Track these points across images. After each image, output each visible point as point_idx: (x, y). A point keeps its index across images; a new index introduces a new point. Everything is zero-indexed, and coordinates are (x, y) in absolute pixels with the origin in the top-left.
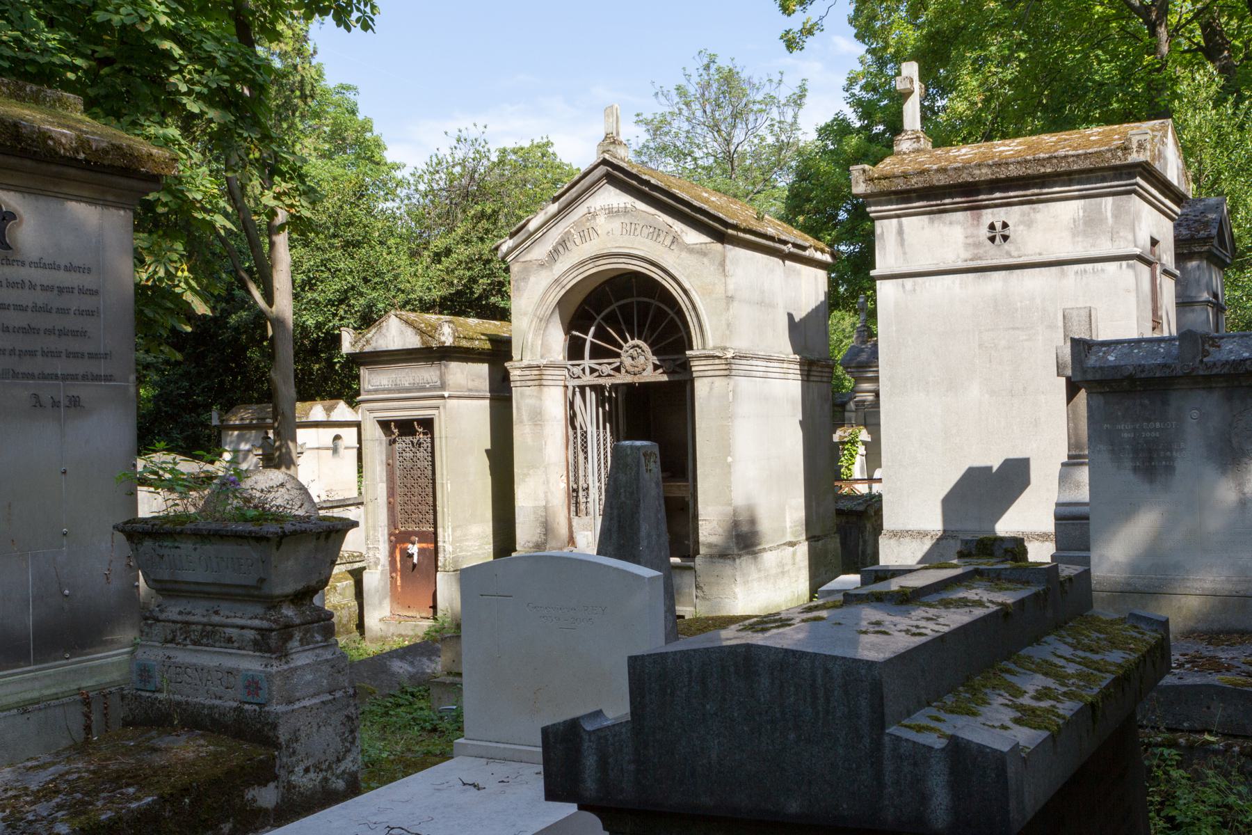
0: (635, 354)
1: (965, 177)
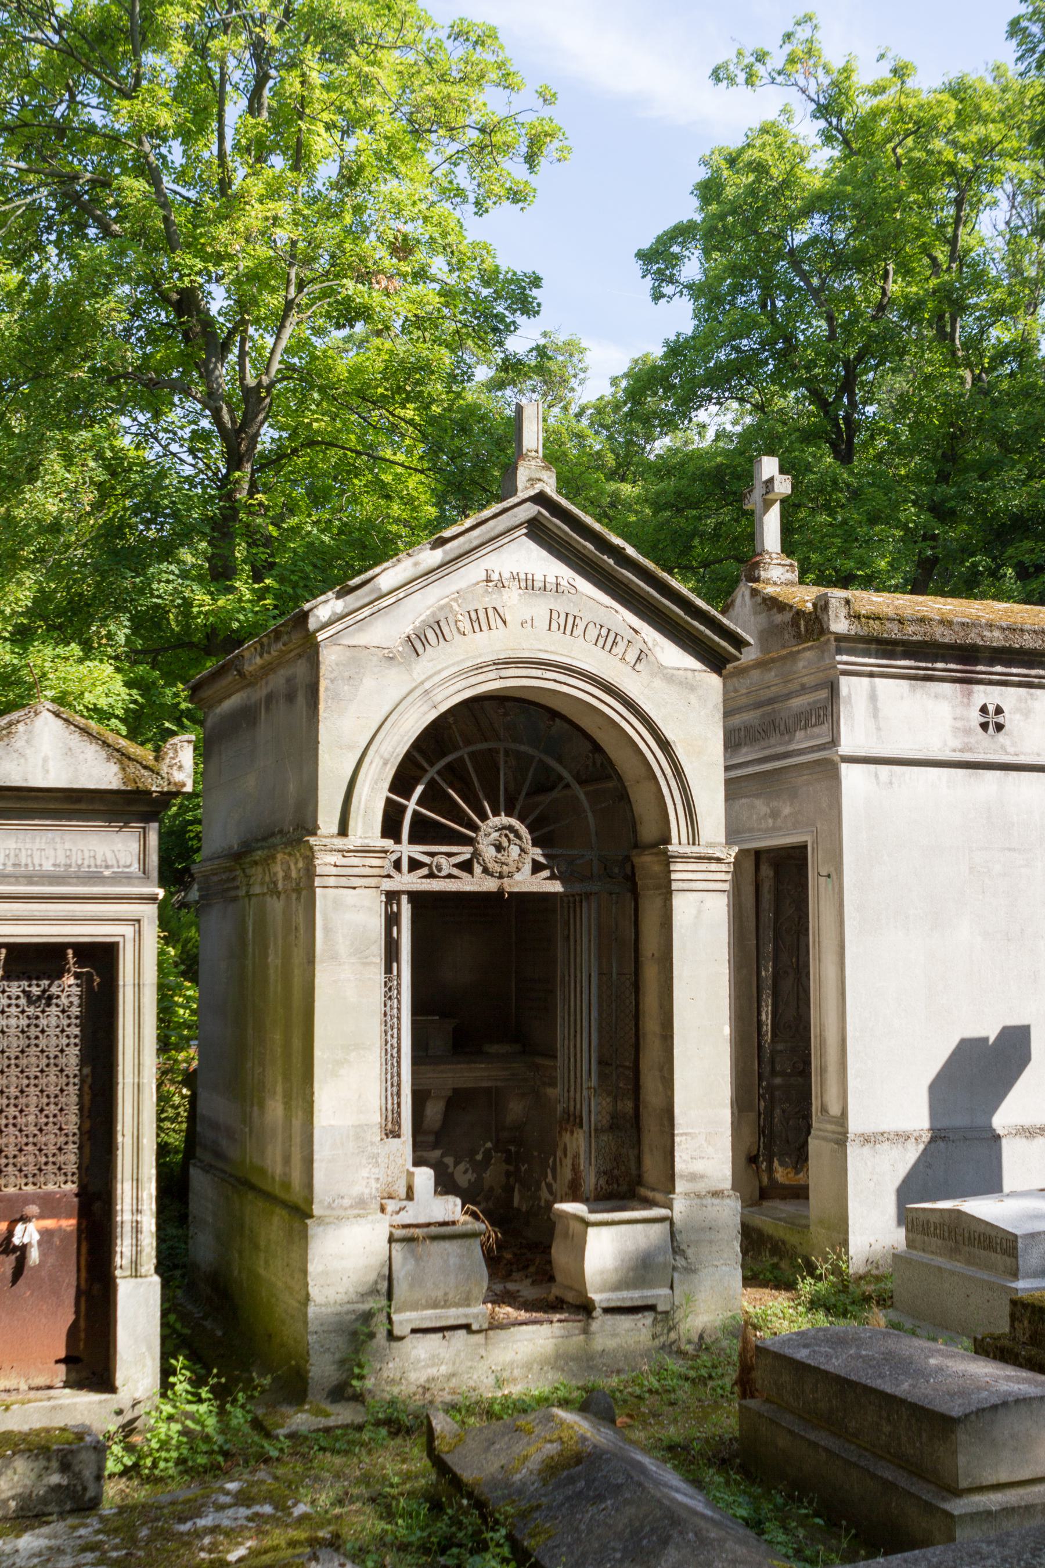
0: (505, 842)
1: (973, 638)
